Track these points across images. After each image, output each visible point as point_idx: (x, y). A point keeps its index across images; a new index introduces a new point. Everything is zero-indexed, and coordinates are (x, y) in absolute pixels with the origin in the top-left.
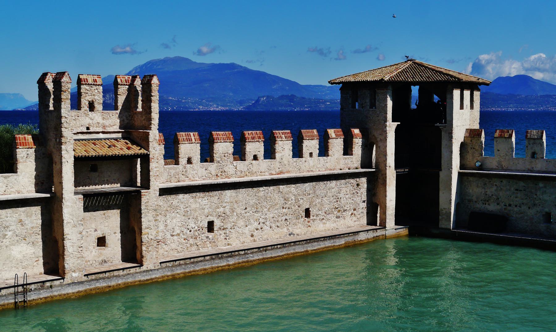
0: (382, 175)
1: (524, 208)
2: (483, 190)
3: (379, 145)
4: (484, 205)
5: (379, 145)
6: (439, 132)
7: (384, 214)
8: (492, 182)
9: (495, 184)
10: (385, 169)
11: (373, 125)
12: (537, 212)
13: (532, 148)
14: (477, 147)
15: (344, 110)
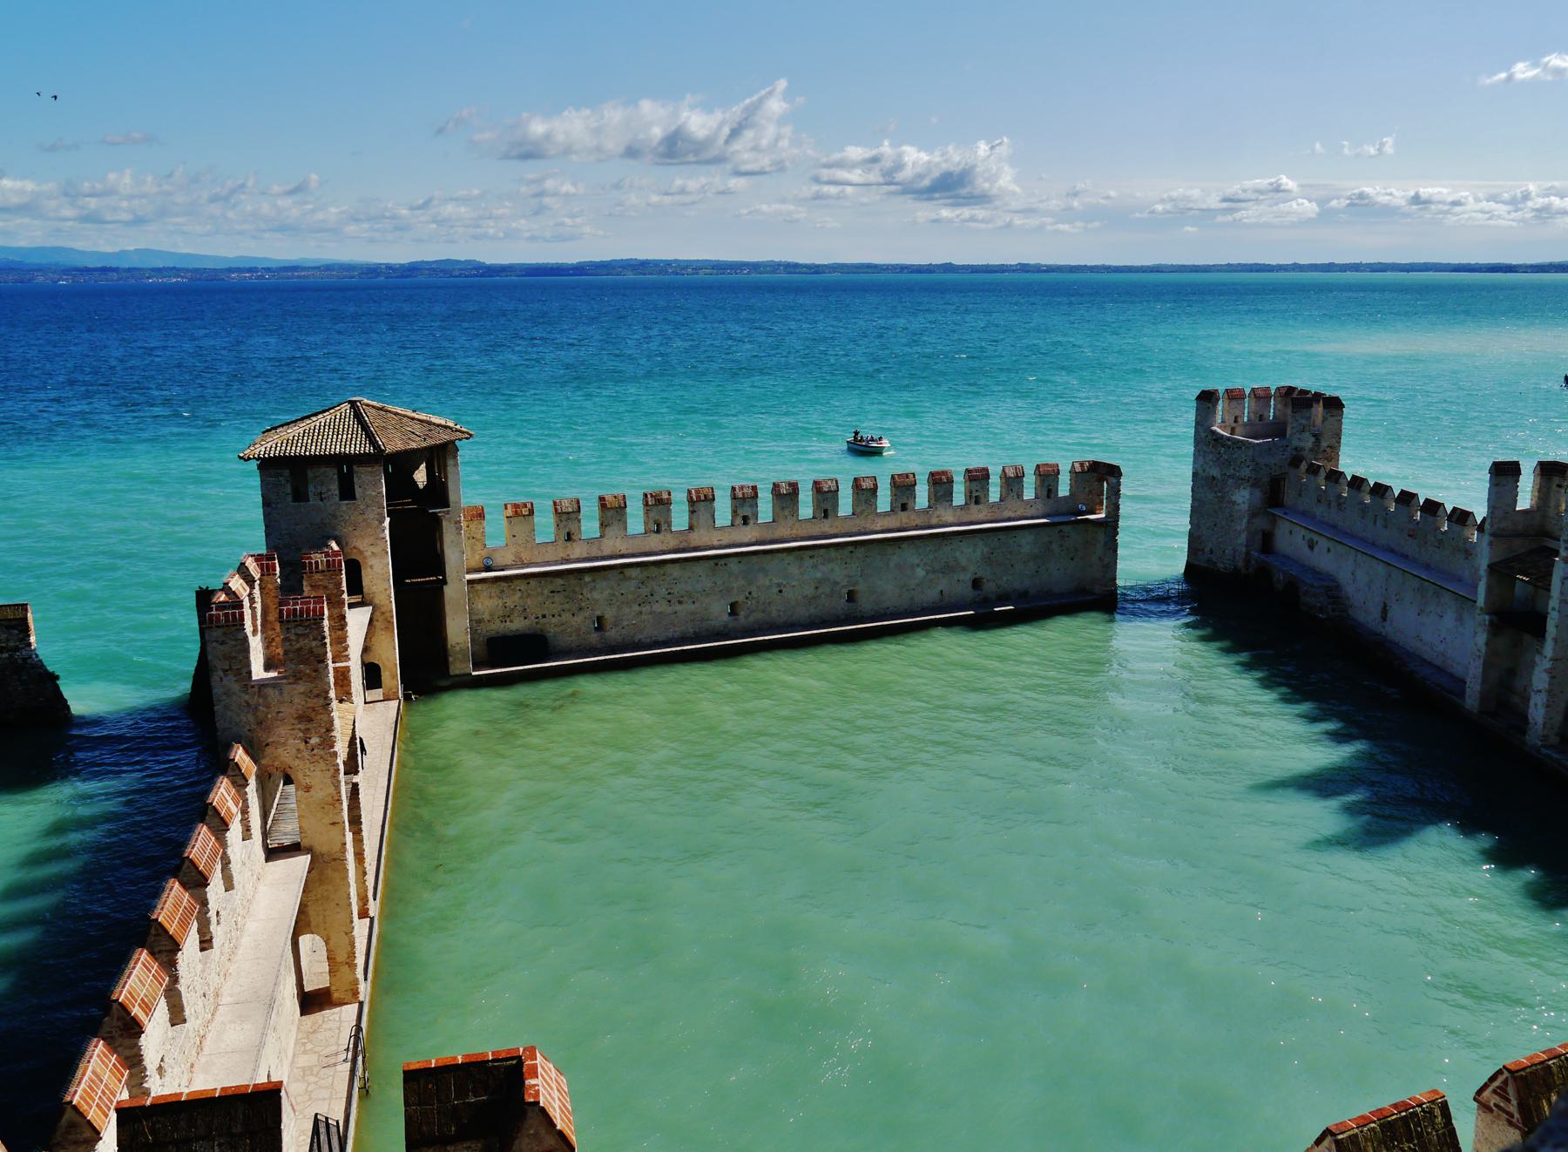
0: (383, 613)
1: (566, 616)
2: (500, 601)
3: (370, 563)
4: (503, 625)
5: (370, 563)
6: (436, 523)
7: (393, 678)
8: (513, 587)
9: (518, 588)
10: (388, 602)
11: (350, 529)
12: (585, 618)
13: (565, 527)
14: (479, 536)
15: (274, 506)
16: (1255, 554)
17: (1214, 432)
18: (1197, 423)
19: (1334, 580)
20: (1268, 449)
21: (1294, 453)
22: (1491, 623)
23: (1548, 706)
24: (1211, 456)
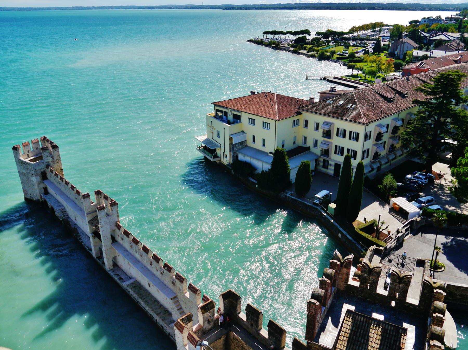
16: (42, 195)
17: (20, 160)
18: (15, 157)
19: (63, 206)
20: (38, 164)
21: (47, 163)
22: (93, 236)
23: (107, 261)
24: (22, 167)
